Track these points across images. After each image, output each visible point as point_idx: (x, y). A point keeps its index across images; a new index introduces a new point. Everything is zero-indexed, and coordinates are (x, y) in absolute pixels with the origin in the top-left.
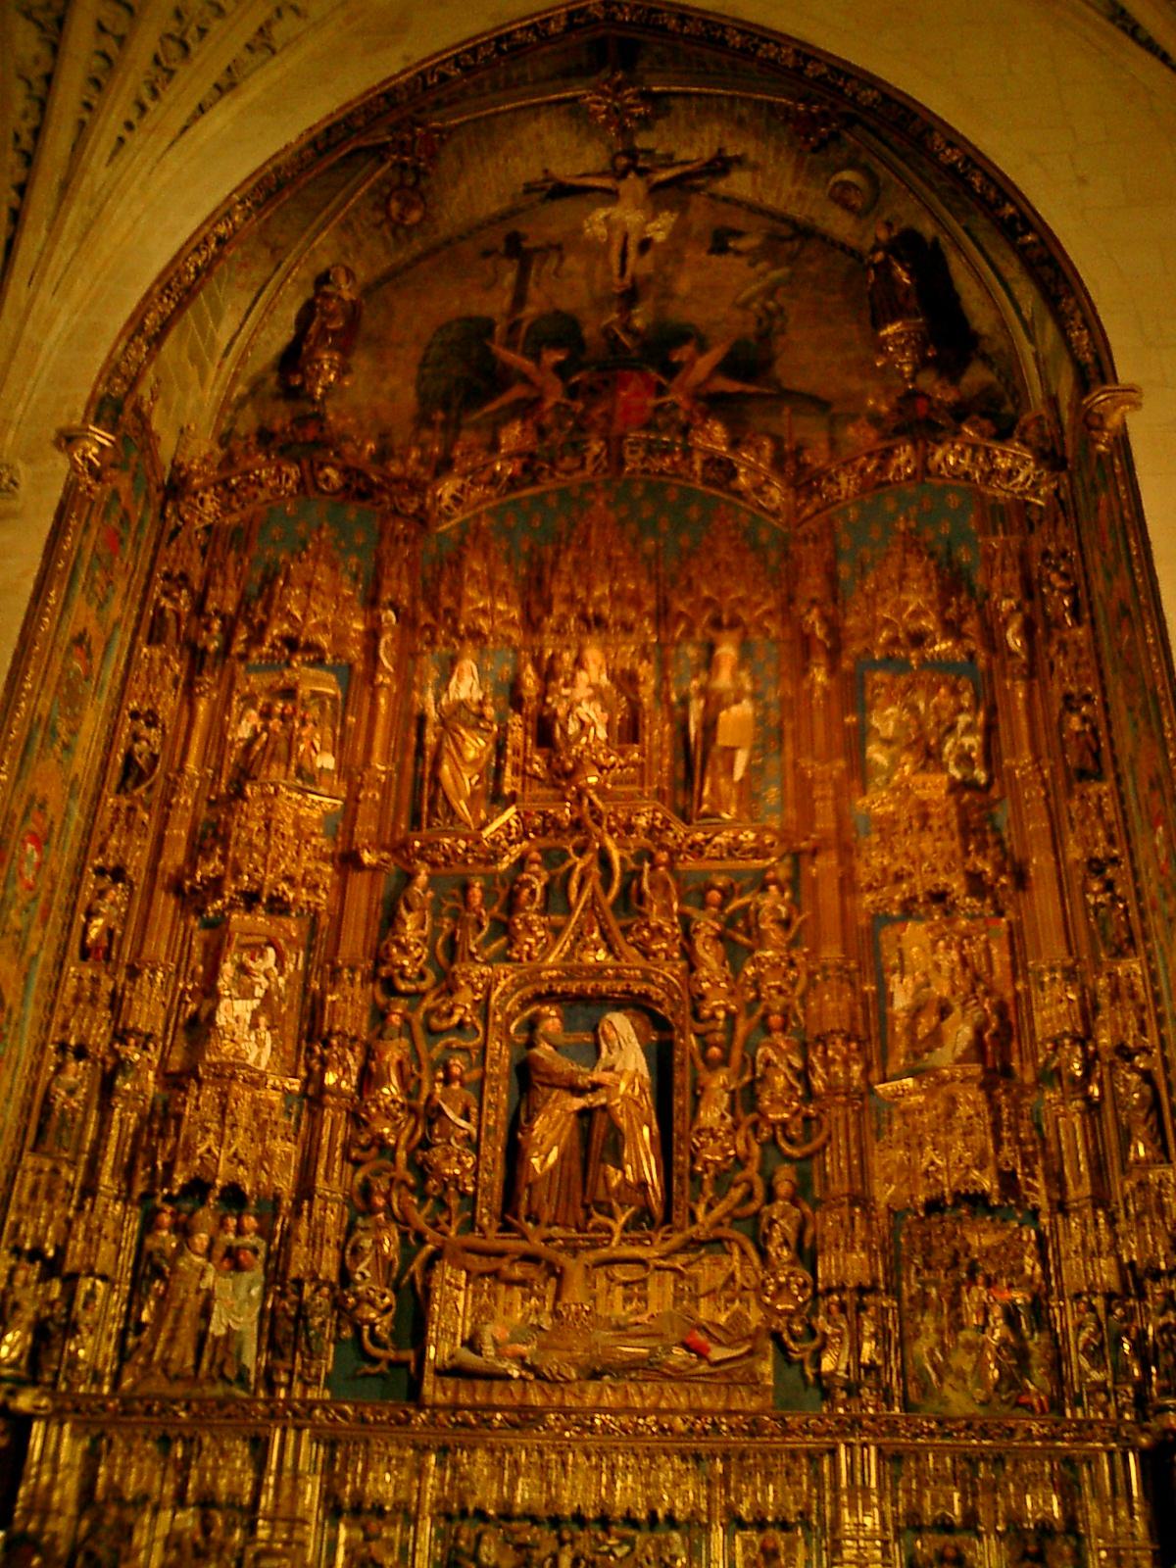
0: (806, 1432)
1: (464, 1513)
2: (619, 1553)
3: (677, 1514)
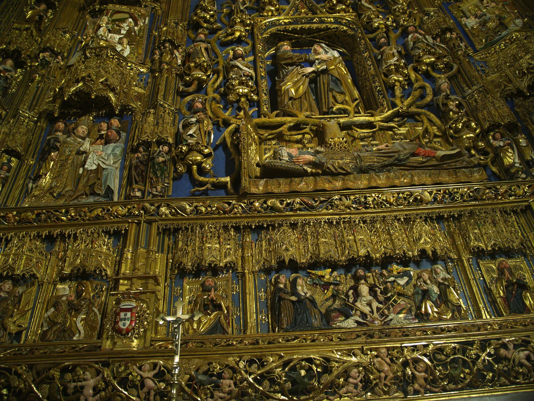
3: (439, 252)
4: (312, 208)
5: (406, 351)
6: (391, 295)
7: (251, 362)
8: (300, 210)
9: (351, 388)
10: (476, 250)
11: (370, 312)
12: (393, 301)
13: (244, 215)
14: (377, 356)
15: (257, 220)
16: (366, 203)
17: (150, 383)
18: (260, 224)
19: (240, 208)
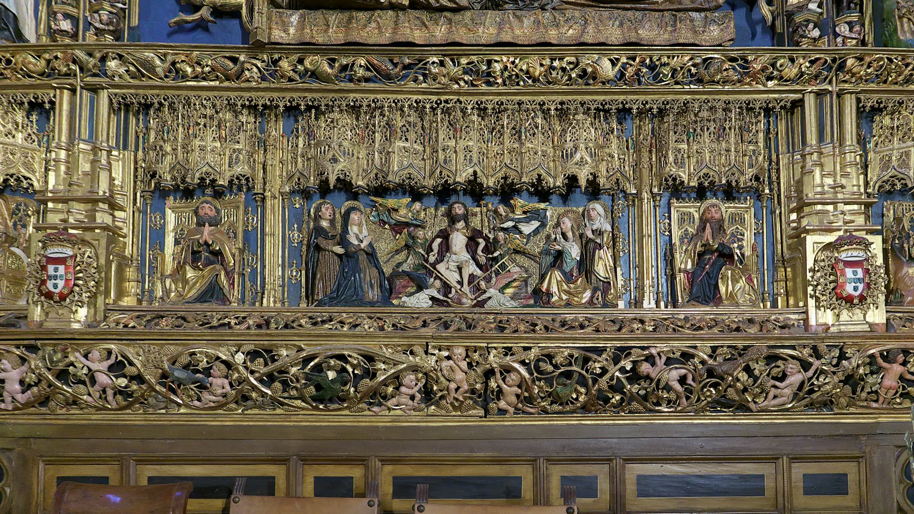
0: (770, 78)
1: (324, 189)
2: (527, 229)
3: (602, 181)
4: (388, 77)
5: (492, 355)
6: (500, 254)
7: (253, 355)
8: (367, 80)
9: (405, 400)
10: (670, 183)
11: (458, 282)
12: (499, 266)
13: (264, 85)
14: (448, 358)
15: (288, 95)
16: (489, 75)
17: (102, 378)
18: (294, 104)
19: (255, 69)
